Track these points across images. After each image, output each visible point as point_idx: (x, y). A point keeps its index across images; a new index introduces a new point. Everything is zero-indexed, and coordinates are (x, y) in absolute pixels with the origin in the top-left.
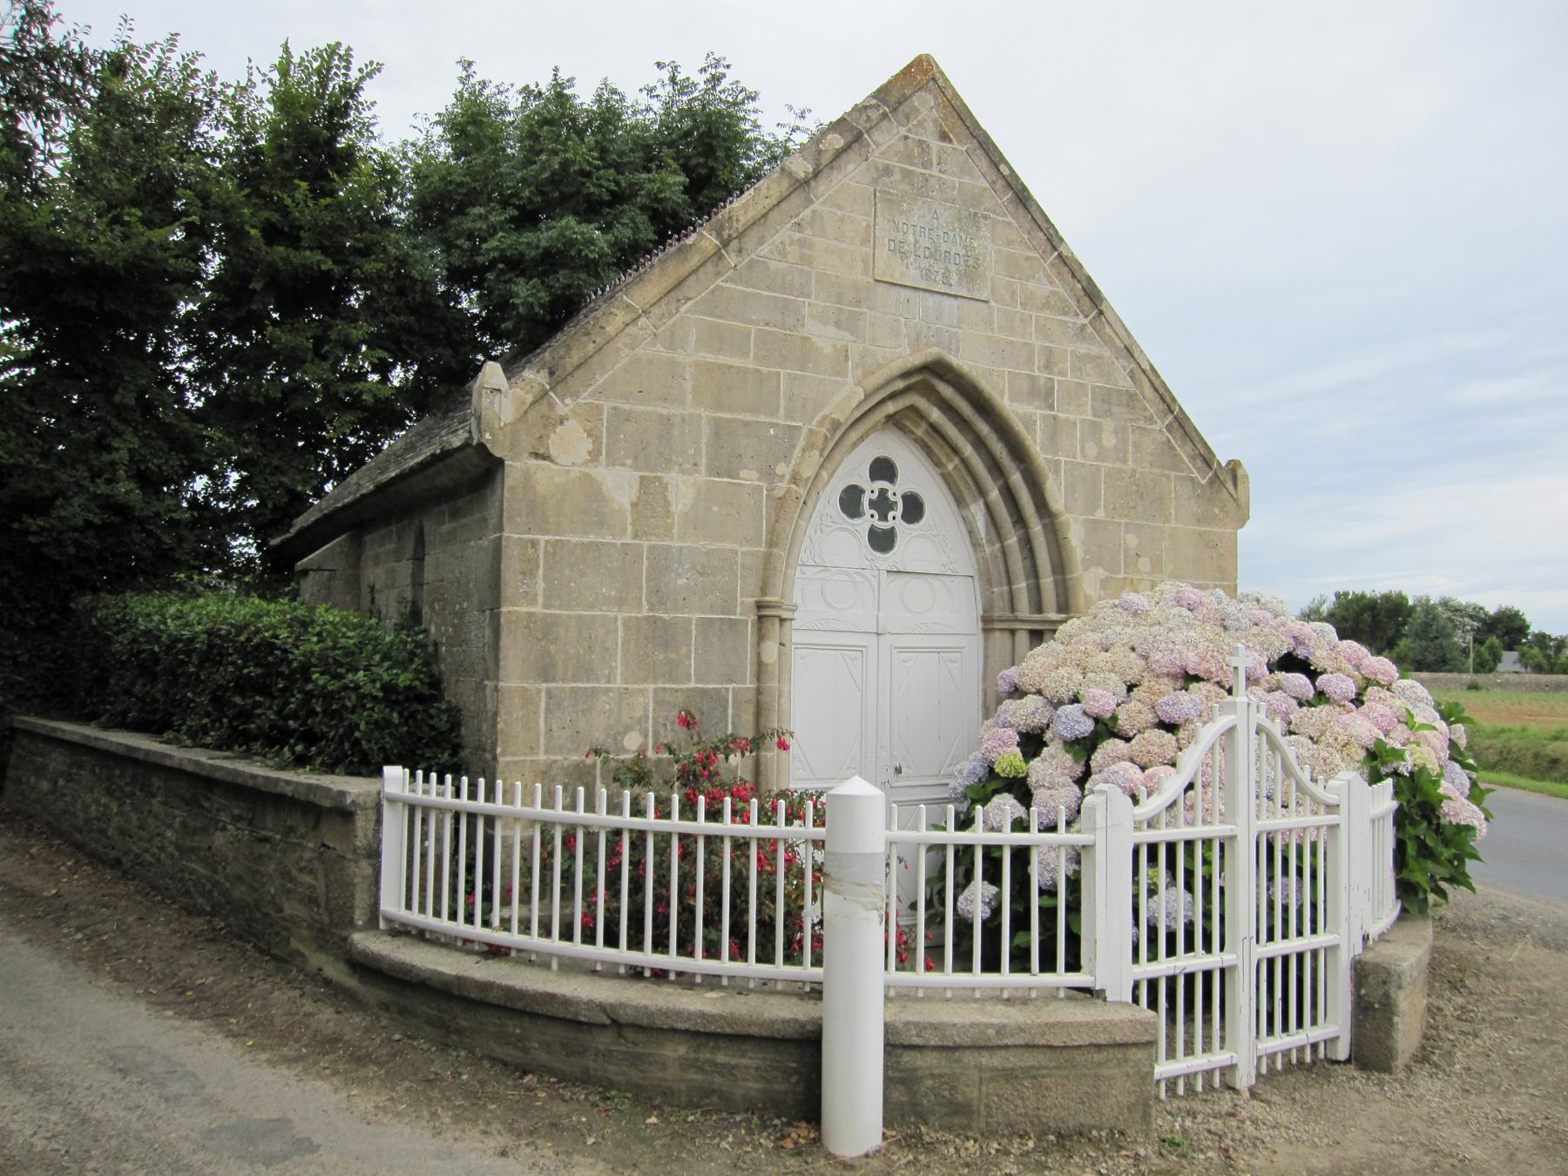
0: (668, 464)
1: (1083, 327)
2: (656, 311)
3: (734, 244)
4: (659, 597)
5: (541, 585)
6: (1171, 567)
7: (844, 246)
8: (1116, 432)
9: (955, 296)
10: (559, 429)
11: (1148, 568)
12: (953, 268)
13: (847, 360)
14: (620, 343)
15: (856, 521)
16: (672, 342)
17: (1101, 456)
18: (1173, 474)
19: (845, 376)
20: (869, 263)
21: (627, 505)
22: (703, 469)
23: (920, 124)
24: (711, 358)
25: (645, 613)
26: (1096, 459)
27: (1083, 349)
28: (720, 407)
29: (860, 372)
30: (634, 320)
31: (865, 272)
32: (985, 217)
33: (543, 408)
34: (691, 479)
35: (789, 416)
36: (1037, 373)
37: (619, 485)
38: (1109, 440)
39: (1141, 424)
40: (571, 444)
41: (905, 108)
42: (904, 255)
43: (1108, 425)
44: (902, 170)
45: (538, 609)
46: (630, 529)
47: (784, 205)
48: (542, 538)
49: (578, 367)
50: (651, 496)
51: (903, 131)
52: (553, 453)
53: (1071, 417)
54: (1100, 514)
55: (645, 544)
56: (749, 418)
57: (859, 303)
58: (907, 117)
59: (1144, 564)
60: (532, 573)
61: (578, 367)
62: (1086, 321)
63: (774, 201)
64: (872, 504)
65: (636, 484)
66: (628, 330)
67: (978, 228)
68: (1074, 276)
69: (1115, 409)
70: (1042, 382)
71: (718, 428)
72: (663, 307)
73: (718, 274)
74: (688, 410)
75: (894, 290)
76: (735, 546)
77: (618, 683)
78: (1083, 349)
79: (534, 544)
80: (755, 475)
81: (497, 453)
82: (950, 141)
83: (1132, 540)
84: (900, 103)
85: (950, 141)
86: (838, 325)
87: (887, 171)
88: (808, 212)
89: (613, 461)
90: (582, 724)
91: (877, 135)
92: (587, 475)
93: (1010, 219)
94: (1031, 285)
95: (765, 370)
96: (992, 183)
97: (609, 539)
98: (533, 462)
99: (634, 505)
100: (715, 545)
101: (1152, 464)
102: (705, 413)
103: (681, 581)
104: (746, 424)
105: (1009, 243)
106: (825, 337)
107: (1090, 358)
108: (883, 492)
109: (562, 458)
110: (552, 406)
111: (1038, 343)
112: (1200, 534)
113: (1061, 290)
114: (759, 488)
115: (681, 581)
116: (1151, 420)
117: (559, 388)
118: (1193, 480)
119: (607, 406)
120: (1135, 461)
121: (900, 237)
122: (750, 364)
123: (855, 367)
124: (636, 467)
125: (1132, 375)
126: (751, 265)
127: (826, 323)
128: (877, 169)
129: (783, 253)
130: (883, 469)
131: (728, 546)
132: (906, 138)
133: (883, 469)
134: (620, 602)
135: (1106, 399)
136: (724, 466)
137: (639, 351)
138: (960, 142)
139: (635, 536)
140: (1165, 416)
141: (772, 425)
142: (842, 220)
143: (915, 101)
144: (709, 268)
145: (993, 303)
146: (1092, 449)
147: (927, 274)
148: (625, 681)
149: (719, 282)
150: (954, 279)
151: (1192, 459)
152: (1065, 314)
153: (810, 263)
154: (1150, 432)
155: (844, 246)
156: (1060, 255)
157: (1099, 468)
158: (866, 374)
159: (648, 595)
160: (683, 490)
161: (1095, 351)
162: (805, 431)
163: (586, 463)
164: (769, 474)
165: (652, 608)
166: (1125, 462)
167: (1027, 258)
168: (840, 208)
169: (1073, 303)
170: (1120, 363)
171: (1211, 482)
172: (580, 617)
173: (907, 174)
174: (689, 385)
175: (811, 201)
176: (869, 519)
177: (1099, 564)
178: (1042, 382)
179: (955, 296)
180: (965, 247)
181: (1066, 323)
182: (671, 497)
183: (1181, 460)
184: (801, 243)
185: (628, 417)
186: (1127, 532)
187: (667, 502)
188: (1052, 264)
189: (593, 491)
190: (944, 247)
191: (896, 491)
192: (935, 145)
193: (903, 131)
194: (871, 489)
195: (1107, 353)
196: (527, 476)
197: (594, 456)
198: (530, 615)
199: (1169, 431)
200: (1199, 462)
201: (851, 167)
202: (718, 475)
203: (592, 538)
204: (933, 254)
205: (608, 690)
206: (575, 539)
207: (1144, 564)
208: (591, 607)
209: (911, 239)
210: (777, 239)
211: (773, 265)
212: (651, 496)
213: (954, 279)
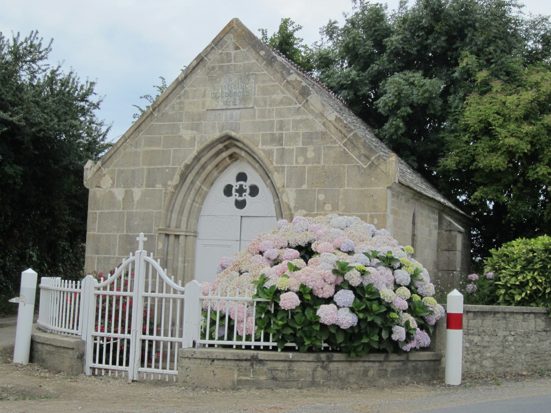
0: (133, 185)
1: (299, 108)
2: (132, 137)
3: (157, 109)
4: (129, 228)
5: (97, 225)
6: (343, 207)
7: (195, 100)
8: (314, 150)
9: (239, 109)
10: (103, 178)
11: (330, 209)
12: (237, 98)
13: (195, 140)
14: (121, 149)
15: (230, 198)
16: (137, 145)
17: (306, 161)
18: (346, 165)
19: (194, 147)
20: (204, 104)
21: (121, 199)
22: (144, 186)
23: (227, 46)
24: (148, 148)
25: (125, 233)
26: (303, 163)
27: (299, 118)
28: (150, 165)
29: (199, 144)
30: (125, 141)
31: (203, 108)
32: (252, 75)
33: (99, 172)
34: (140, 189)
35: (173, 164)
36: (275, 132)
37: (119, 193)
38: (310, 154)
39: (329, 145)
40: (106, 182)
41: (221, 42)
42: (217, 98)
43: (310, 148)
44: (219, 66)
45: (96, 233)
46: (122, 207)
47: (174, 91)
48: (98, 211)
49: (109, 158)
50: (128, 196)
51: (220, 51)
52: (102, 186)
53: (291, 148)
54: (305, 187)
55: (126, 211)
56: (160, 167)
57: (200, 119)
58: (222, 46)
59: (328, 207)
60: (95, 222)
61: (109, 158)
62: (301, 105)
63: (170, 91)
64: (237, 191)
65: (124, 193)
66: (124, 144)
67: (249, 80)
68: (294, 88)
69: (314, 141)
70: (277, 135)
71: (149, 170)
72: (134, 135)
73: (151, 121)
74: (141, 167)
75: (214, 112)
76: (153, 210)
77: (117, 256)
78: (299, 118)
79: (96, 213)
80: (161, 186)
81: (87, 187)
82: (240, 49)
83: (322, 197)
84: (219, 42)
85: (240, 49)
86: (192, 129)
87: (213, 68)
88: (183, 91)
89: (117, 187)
90: (106, 268)
91: (210, 56)
92: (110, 191)
93: (265, 72)
94: (274, 96)
95: (166, 149)
96: (257, 60)
97: (116, 211)
98: (97, 189)
99: (123, 199)
100: (147, 210)
101: (334, 162)
102: (146, 167)
103: (136, 223)
104: (158, 169)
105: (264, 82)
106: (186, 134)
107: (302, 121)
108: (241, 186)
109: (104, 187)
110: (102, 171)
111: (276, 119)
112: (362, 191)
113: (289, 95)
114: (162, 190)
115: (136, 223)
116: (335, 142)
117: (104, 166)
118: (358, 167)
119: (117, 169)
120: (325, 162)
121: (216, 92)
122: (161, 148)
123: (198, 142)
124: (124, 187)
125: (324, 124)
126: (162, 115)
127: (188, 129)
128: (209, 69)
129: (173, 108)
130: (242, 177)
131: (151, 210)
132: (221, 53)
133: (242, 177)
134: (118, 230)
135: (309, 138)
136: (151, 184)
137: (127, 150)
138: (243, 48)
139: (123, 209)
140: (343, 139)
141: (167, 168)
142: (195, 91)
143: (225, 39)
144: (149, 119)
145: (256, 108)
146: (301, 159)
147: (226, 103)
148: (119, 255)
149: (152, 123)
150: (238, 102)
151: (359, 157)
152: (290, 104)
153: (183, 109)
154: (333, 148)
155: (195, 100)
156: (287, 81)
157: (304, 167)
158: (201, 144)
159: (127, 227)
160: (137, 193)
161: (305, 117)
162: (178, 169)
163: (110, 188)
164: (165, 185)
165: (127, 232)
166: (319, 163)
167: (272, 86)
168: (194, 87)
169: (294, 99)
170: (317, 121)
171: (370, 166)
172: (107, 235)
173: (221, 67)
174: (141, 159)
175: (184, 87)
176: (235, 196)
177: (302, 209)
178: (277, 135)
179: (239, 109)
180: (243, 89)
181: (290, 109)
182: (134, 196)
183: (352, 158)
184: (180, 103)
185: (122, 172)
186: (319, 193)
187: (133, 198)
188: (284, 86)
189: (112, 195)
190: (234, 91)
191: (246, 185)
192: (233, 52)
193: (220, 51)
194: (236, 185)
195: (311, 117)
196: (95, 193)
197: (113, 185)
198: (94, 235)
199: (345, 146)
200: (363, 158)
201: (199, 71)
202: (149, 187)
203: (111, 211)
204: (230, 94)
205: (114, 257)
206: (106, 211)
207: (328, 207)
208: (110, 232)
209: (220, 91)
210: (172, 104)
211: (170, 113)
212: (128, 196)
213: (238, 102)
